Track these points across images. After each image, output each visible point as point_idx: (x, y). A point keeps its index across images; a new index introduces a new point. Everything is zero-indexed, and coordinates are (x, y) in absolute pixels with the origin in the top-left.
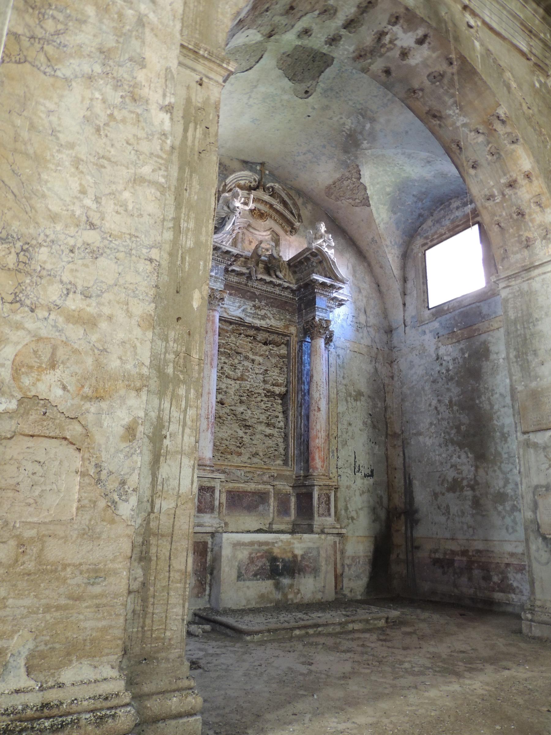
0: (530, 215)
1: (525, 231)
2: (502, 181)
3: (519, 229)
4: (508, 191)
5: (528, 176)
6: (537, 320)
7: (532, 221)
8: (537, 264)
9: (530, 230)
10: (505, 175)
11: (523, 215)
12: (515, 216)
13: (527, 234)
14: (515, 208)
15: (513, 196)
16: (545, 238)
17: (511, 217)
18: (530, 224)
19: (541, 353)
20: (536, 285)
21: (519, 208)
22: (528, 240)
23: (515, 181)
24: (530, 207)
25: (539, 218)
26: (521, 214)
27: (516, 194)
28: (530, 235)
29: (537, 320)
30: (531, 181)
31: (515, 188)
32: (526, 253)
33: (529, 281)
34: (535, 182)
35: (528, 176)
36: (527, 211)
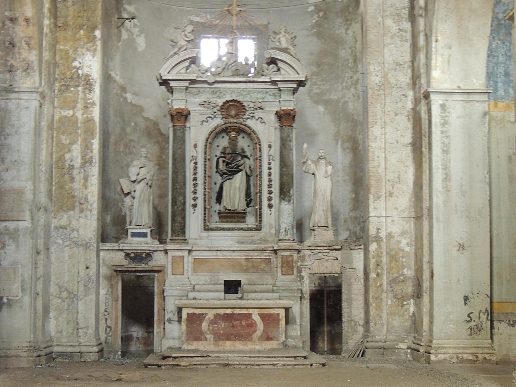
0: (19, 48)
1: (12, 58)
2: (7, 14)
3: (7, 55)
4: (8, 23)
5: (27, 20)
6: (8, 135)
7: (20, 53)
8: (16, 90)
9: (15, 60)
10: (11, 10)
11: (14, 46)
12: (7, 43)
13: (12, 62)
14: (9, 38)
15: (11, 29)
16: (25, 70)
17: (4, 43)
18: (17, 56)
19: (7, 161)
20: (12, 106)
21: (12, 39)
22: (12, 66)
23: (16, 19)
24: (21, 43)
25: (25, 54)
26: (12, 44)
27: (14, 28)
28: (15, 64)
29: (8, 135)
30: (28, 25)
31: (14, 24)
32: (8, 76)
33: (8, 101)
34: (31, 28)
35: (27, 20)
36: (18, 45)
